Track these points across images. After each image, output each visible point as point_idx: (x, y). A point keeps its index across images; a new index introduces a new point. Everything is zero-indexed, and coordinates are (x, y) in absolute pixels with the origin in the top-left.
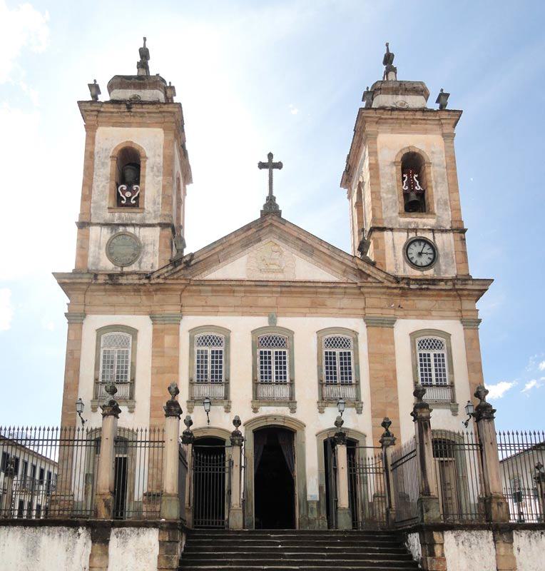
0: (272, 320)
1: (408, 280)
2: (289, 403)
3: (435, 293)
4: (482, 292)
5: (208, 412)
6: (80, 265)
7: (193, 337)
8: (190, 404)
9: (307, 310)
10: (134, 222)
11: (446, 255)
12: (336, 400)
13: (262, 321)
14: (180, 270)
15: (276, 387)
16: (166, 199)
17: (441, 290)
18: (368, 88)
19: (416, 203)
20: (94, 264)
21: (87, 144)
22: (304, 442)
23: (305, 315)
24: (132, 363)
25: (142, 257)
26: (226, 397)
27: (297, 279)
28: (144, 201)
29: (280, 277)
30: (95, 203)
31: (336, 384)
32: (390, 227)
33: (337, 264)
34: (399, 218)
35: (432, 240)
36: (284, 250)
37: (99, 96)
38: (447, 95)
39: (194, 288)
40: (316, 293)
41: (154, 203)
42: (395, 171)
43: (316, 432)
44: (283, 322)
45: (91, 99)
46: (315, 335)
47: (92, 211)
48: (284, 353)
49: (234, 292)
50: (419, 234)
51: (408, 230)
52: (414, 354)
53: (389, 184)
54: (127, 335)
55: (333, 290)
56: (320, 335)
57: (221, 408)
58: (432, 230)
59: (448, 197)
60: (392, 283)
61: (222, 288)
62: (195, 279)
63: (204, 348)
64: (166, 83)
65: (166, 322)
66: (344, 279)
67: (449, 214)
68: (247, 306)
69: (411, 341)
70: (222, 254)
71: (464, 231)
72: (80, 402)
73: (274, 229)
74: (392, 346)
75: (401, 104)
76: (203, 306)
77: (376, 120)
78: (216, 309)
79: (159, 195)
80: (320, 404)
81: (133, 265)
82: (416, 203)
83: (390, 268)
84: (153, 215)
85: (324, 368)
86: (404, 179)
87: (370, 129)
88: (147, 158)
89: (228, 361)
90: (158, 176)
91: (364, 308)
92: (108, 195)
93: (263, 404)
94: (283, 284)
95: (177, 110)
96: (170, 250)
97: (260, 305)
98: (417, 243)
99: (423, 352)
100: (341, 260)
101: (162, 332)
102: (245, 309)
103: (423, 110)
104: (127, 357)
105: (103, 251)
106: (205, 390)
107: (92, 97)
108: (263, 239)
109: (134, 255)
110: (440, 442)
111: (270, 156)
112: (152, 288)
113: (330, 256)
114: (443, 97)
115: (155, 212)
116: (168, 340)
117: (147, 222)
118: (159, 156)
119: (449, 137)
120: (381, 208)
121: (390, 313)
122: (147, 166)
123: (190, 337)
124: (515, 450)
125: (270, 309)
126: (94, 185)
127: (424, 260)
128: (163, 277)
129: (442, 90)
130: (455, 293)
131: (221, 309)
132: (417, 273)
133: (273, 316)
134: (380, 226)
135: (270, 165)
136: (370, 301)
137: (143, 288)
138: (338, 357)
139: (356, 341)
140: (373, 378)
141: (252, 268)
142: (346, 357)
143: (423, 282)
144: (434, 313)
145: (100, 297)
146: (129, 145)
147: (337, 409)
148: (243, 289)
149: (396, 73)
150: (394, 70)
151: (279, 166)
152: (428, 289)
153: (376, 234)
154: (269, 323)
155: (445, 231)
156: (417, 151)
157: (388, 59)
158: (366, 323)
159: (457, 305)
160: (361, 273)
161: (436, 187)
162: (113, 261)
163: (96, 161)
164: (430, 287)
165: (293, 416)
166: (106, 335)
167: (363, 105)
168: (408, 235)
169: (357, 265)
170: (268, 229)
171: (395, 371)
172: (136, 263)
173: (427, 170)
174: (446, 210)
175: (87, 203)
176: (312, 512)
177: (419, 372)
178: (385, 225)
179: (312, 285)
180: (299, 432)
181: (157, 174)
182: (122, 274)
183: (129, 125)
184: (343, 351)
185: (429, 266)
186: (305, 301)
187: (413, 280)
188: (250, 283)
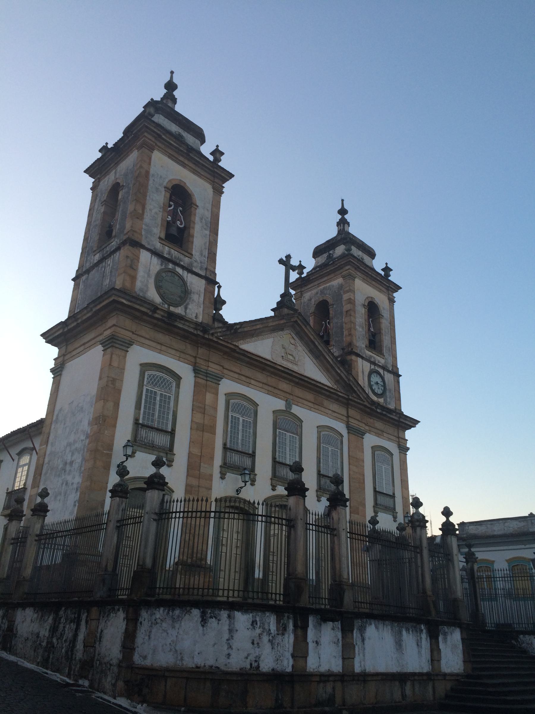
0: (289, 406)
3: (388, 419)
4: (410, 427)
8: (223, 469)
17: (392, 419)
20: (141, 290)
23: (310, 408)
25: (188, 304)
28: (192, 248)
29: (295, 368)
30: (146, 225)
33: (334, 373)
35: (383, 375)
41: (201, 254)
44: (296, 410)
50: (376, 368)
53: (361, 320)
54: (171, 380)
56: (320, 430)
63: (237, 415)
65: (208, 379)
66: (335, 387)
68: (272, 386)
77: (356, 267)
79: (206, 249)
80: (319, 493)
81: (180, 308)
84: (200, 265)
92: (160, 224)
94: (303, 378)
97: (280, 388)
100: (339, 372)
102: (270, 389)
105: (152, 281)
108: (285, 329)
113: (331, 365)
116: (209, 397)
117: (194, 269)
121: (363, 427)
122: (197, 215)
123: (226, 400)
125: (288, 395)
131: (253, 382)
146: (182, 184)
148: (272, 370)
152: (385, 415)
153: (354, 357)
158: (348, 430)
161: (385, 335)
166: (150, 372)
168: (371, 367)
169: (349, 380)
178: (358, 352)
181: (205, 227)
183: (184, 165)
186: (310, 396)
188: (280, 368)
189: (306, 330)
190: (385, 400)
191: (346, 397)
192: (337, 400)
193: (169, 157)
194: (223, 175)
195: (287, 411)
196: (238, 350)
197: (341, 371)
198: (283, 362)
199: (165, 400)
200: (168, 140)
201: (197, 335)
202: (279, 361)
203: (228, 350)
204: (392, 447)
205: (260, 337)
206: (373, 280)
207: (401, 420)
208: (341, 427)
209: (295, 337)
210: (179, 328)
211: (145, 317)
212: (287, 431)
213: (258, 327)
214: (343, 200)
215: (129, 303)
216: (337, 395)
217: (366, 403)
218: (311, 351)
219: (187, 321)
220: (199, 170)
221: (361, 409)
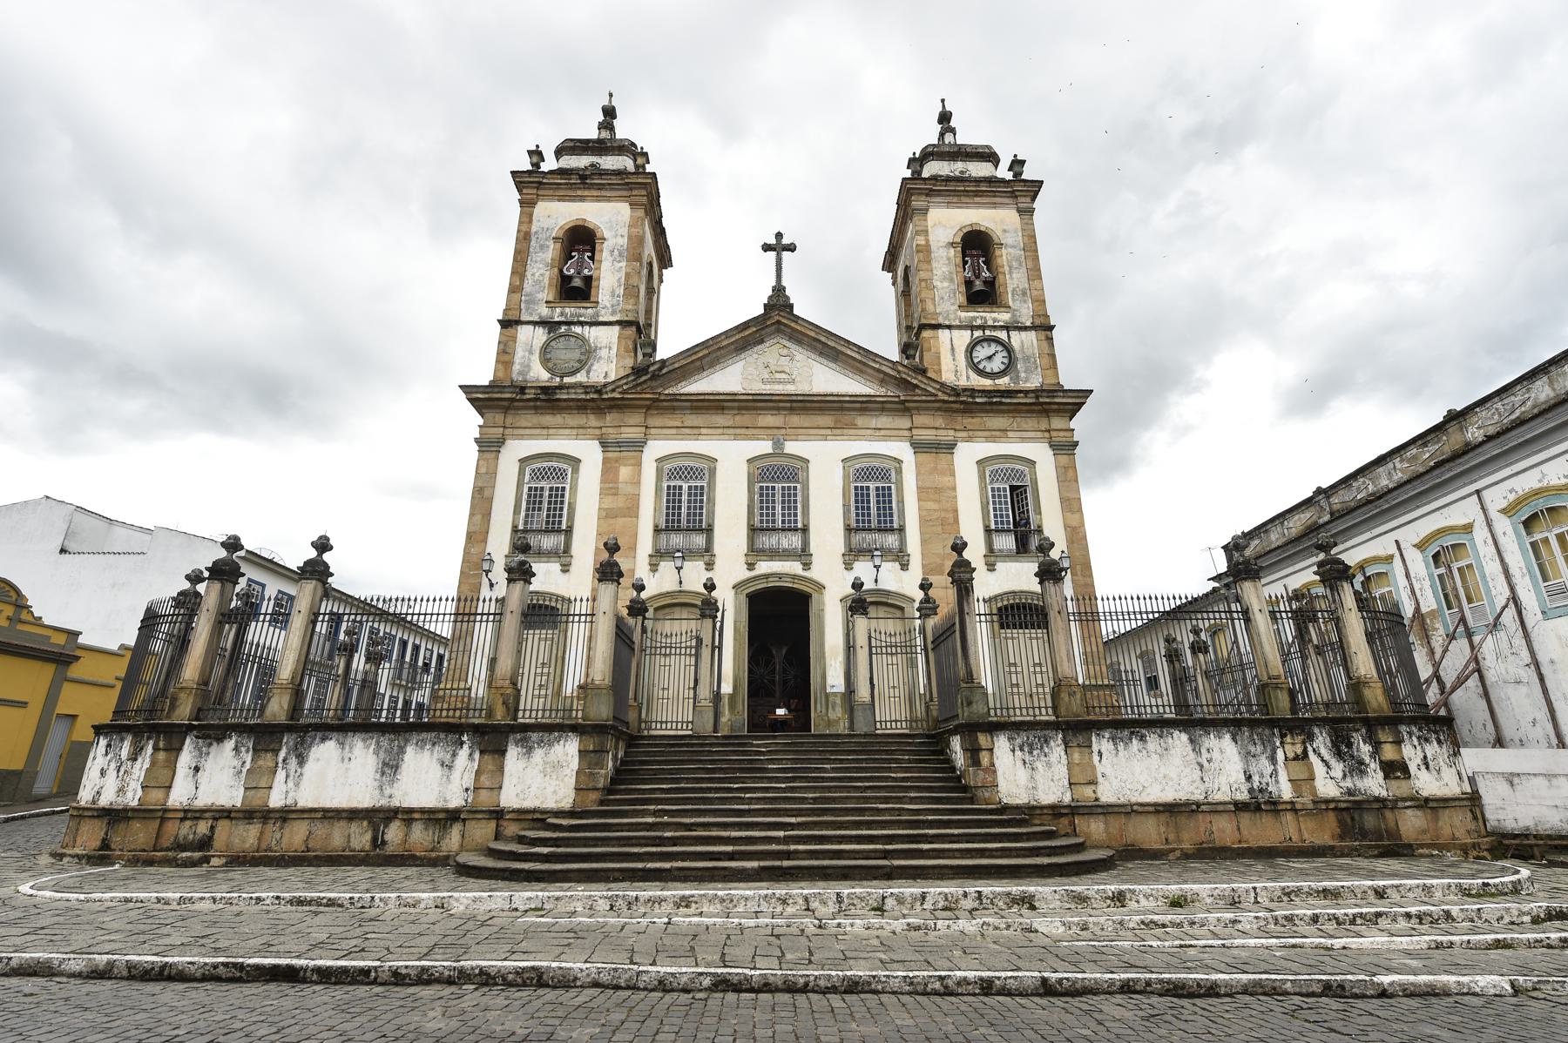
0: (778, 444)
1: (972, 392)
2: (800, 556)
5: (679, 569)
6: (501, 374)
7: (662, 469)
9: (828, 432)
10: (582, 319)
11: (1027, 359)
12: (870, 551)
13: (765, 447)
14: (645, 381)
15: (782, 535)
16: (630, 291)
18: (914, 154)
19: (982, 294)
20: (520, 373)
21: (520, 223)
22: (823, 610)
24: (569, 503)
25: (592, 365)
26: (709, 548)
27: (815, 390)
29: (790, 389)
31: (870, 530)
32: (947, 323)
33: (870, 371)
34: (959, 313)
36: (795, 353)
37: (542, 164)
38: (1022, 163)
39: (665, 404)
40: (842, 409)
41: (613, 296)
42: (954, 254)
43: (840, 597)
44: (791, 447)
45: (530, 168)
46: (841, 465)
47: (523, 306)
48: (795, 488)
49: (723, 408)
50: (988, 333)
51: (972, 328)
52: (983, 489)
55: (865, 405)
57: (701, 564)
58: (1007, 328)
59: (1027, 286)
60: (949, 395)
61: (706, 404)
62: (666, 392)
64: (636, 148)
66: (882, 391)
67: (1028, 308)
69: (979, 471)
70: (707, 359)
71: (1051, 328)
72: (488, 557)
73: (782, 327)
74: (951, 478)
75: (962, 172)
76: (677, 427)
78: (696, 431)
80: (847, 558)
82: (982, 294)
83: (948, 377)
85: (853, 509)
86: (965, 263)
87: (917, 202)
88: (605, 239)
89: (712, 501)
90: (620, 262)
91: (910, 429)
93: (765, 558)
94: (794, 398)
95: (650, 181)
96: (633, 354)
98: (985, 344)
99: (996, 486)
100: (877, 366)
101: (617, 461)
102: (738, 431)
103: (991, 180)
104: (563, 496)
105: (536, 358)
106: (677, 540)
107: (532, 165)
109: (579, 361)
110: (1031, 609)
111: (779, 236)
112: (603, 405)
113: (860, 362)
114: (1017, 164)
115: (613, 306)
116: (625, 472)
117: (601, 319)
118: (622, 236)
119: (1027, 213)
120: (934, 299)
121: (947, 435)
124: (1142, 619)
126: (528, 274)
127: (997, 365)
128: (620, 390)
129: (1015, 156)
130: (1040, 407)
131: (704, 431)
132: (986, 383)
133: (779, 440)
134: (933, 322)
135: (779, 247)
136: (920, 419)
137: (591, 404)
138: (873, 493)
139: (899, 471)
140: (924, 521)
141: (750, 377)
142: (884, 495)
143: (992, 394)
144: (1010, 434)
145: (527, 419)
146: (581, 223)
147: (870, 564)
148: (736, 404)
149: (955, 135)
150: (953, 131)
151: (791, 248)
152: (1001, 403)
153: (926, 334)
154: (774, 449)
155: (1025, 328)
156: (983, 229)
157: (945, 118)
158: (914, 448)
159: (1044, 425)
160: (904, 384)
161: (1010, 273)
162: (549, 370)
163: (533, 243)
164: (1004, 400)
165: (806, 574)
166: (534, 466)
167: (908, 174)
169: (899, 372)
170: (773, 327)
171: (956, 511)
172: (583, 372)
173: (997, 252)
174: (1025, 302)
175: (516, 296)
176: (834, 709)
177: (992, 513)
178: (941, 320)
179: (836, 399)
180: (815, 596)
182: (561, 387)
183: (582, 199)
184: (880, 485)
185: (1002, 373)
187: (979, 391)
189: (798, 328)
190: (1016, 379)
191: (897, 399)
192: (883, 410)
193: (559, 200)
194: (640, 180)
195: (778, 452)
196: (662, 398)
197: (881, 364)
198: (763, 387)
199: (558, 494)
200: (552, 181)
201: (593, 400)
202: (757, 387)
203: (648, 403)
204: (1040, 453)
205: (718, 367)
206: (976, 196)
207: (1041, 400)
208: (901, 450)
209: (788, 344)
210: (565, 400)
211: (516, 404)
212: (773, 480)
213: (700, 355)
214: (943, 101)
215: (487, 396)
216: (876, 402)
217: (942, 396)
218: (821, 354)
219: (568, 388)
220: (603, 193)
221: (939, 409)
